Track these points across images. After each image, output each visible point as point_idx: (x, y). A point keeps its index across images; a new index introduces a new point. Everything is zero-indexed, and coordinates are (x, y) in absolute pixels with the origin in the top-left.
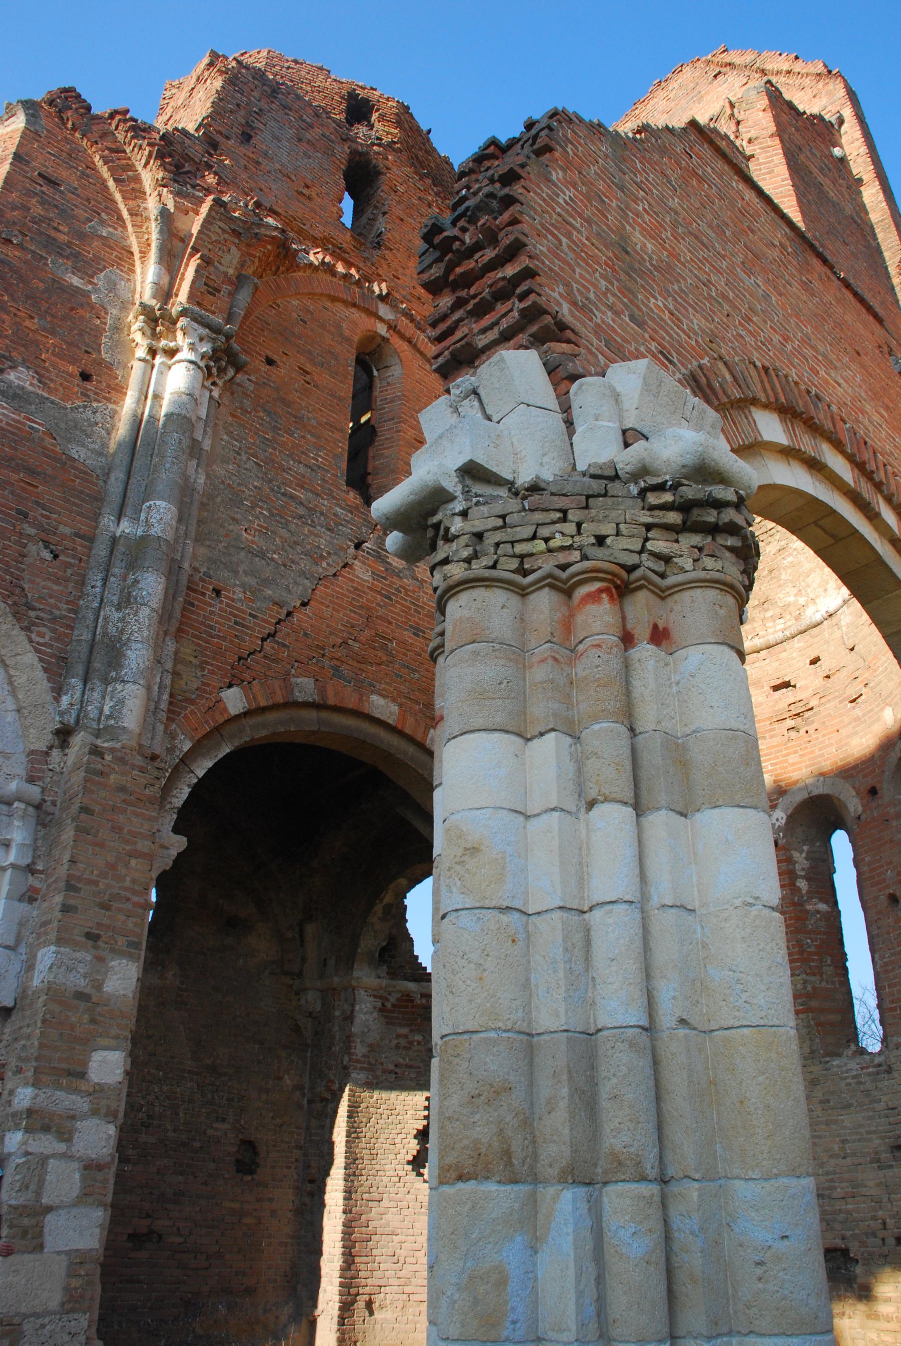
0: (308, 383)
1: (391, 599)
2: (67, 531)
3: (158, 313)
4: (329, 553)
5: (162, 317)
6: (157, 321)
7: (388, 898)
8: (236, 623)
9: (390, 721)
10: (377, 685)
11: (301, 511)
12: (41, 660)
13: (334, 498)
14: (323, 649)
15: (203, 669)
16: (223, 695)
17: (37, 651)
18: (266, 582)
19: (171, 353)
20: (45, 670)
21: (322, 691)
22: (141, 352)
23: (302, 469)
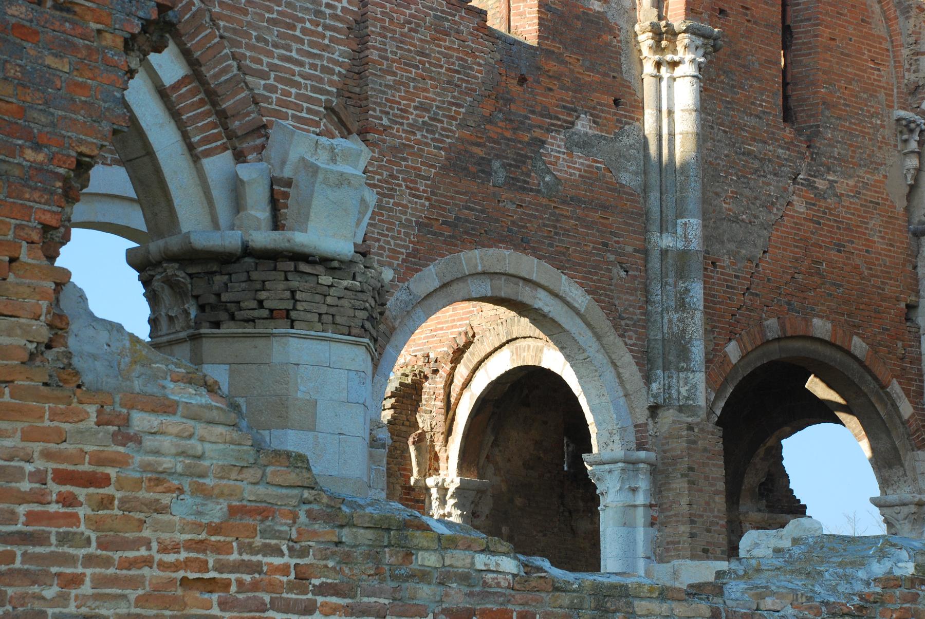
0: (749, 21)
1: (819, 223)
2: (629, 249)
3: (664, 30)
4: (777, 198)
5: (666, 32)
6: (663, 35)
7: (770, 442)
8: (728, 287)
9: (827, 339)
10: (815, 308)
11: (756, 164)
12: (634, 357)
13: (777, 140)
14: (779, 288)
15: (713, 332)
16: (727, 349)
17: (631, 351)
18: (741, 244)
19: (674, 64)
20: (637, 364)
21: (783, 327)
22: (649, 68)
23: (753, 121)
